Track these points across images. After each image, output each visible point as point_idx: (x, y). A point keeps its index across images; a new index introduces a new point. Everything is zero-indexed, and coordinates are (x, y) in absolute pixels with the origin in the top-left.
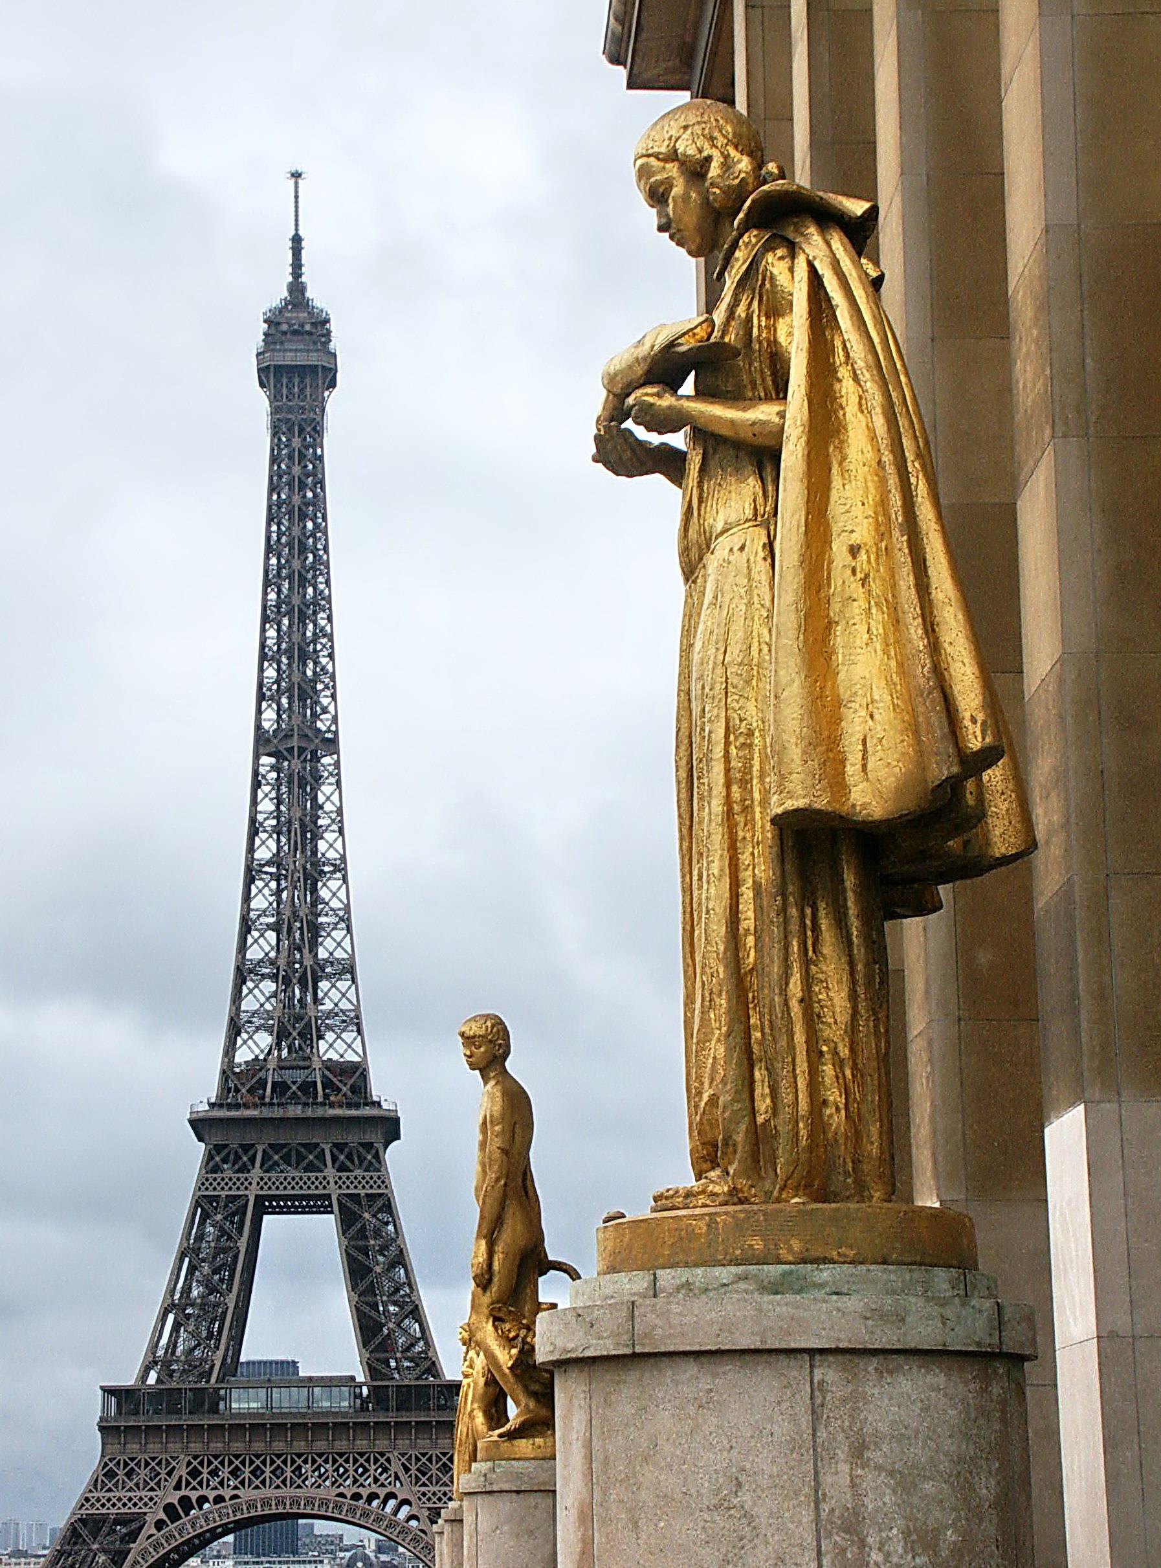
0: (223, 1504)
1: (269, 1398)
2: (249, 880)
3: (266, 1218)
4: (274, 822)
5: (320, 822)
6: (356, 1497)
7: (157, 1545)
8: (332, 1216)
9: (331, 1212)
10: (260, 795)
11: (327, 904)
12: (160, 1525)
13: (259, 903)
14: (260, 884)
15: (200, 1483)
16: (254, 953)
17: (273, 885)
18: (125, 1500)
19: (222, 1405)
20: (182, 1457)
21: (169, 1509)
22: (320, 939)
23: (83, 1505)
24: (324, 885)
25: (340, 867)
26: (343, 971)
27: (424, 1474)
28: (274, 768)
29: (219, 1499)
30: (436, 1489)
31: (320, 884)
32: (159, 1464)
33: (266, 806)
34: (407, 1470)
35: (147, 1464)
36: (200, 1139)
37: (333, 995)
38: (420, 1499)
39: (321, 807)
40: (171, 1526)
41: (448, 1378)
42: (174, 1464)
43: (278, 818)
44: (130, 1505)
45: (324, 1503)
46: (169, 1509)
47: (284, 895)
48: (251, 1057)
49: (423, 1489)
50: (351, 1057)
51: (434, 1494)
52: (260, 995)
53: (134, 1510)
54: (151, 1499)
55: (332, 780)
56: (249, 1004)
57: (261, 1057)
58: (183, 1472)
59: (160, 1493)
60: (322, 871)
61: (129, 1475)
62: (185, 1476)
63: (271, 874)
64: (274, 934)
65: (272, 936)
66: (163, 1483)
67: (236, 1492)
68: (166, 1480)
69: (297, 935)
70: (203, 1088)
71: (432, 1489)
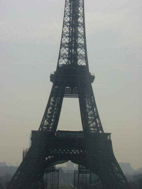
2: (63, 26)
3: (64, 98)
4: (69, 14)
5: (79, 14)
8: (78, 98)
9: (79, 97)
10: (66, 9)
11: (79, 32)
13: (65, 31)
14: (65, 27)
16: (64, 42)
17: (69, 27)
22: (78, 40)
24: (80, 27)
25: (83, 25)
26: (83, 47)
28: (70, 2)
31: (79, 28)
33: (67, 10)
36: (51, 80)
37: (80, 51)
39: (79, 11)
41: (105, 132)
43: (70, 13)
47: (71, 29)
48: (62, 64)
50: (84, 64)
52: (65, 51)
55: (81, 6)
56: (62, 53)
57: (65, 64)
60: (79, 26)
63: (68, 25)
64: (69, 38)
65: (68, 38)
69: (73, 38)
70: (53, 69)
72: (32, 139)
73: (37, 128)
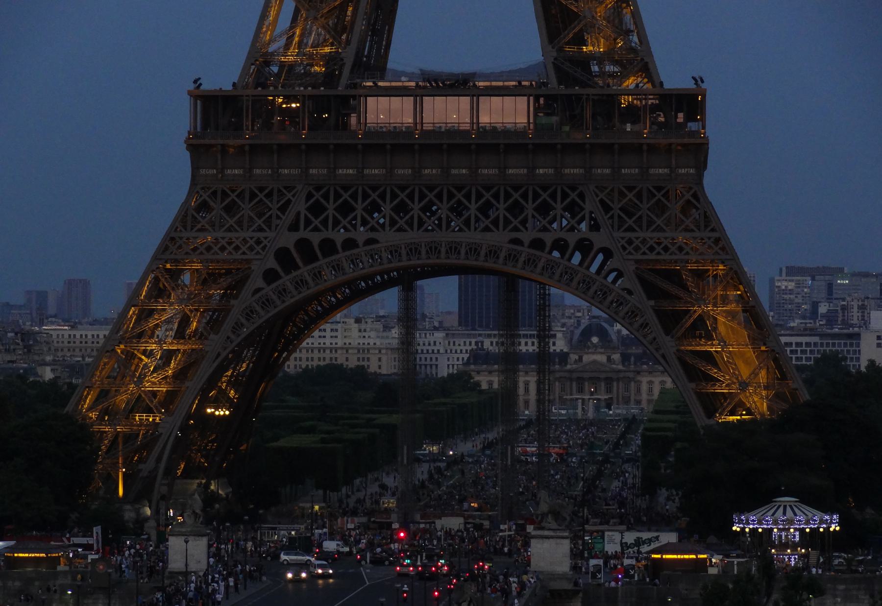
0: (356, 251)
1: (418, 110)
6: (538, 244)
7: (266, 303)
12: (270, 276)
15: (325, 222)
18: (224, 242)
19: (353, 120)
20: (299, 187)
21: (283, 255)
23: (166, 249)
27: (630, 215)
29: (350, 244)
30: (648, 234)
32: (269, 195)
34: (607, 208)
35: (253, 196)
38: (624, 248)
40: (286, 280)
42: (289, 196)
44: (230, 248)
45: (493, 253)
46: (283, 255)
49: (629, 235)
51: (644, 241)
53: (238, 256)
54: (258, 242)
58: (300, 206)
59: (271, 234)
61: (230, 209)
62: (303, 212)
66: (275, 221)
67: (372, 235)
68: (278, 217)
71: (641, 234)
72: (197, 149)
73: (224, 77)
